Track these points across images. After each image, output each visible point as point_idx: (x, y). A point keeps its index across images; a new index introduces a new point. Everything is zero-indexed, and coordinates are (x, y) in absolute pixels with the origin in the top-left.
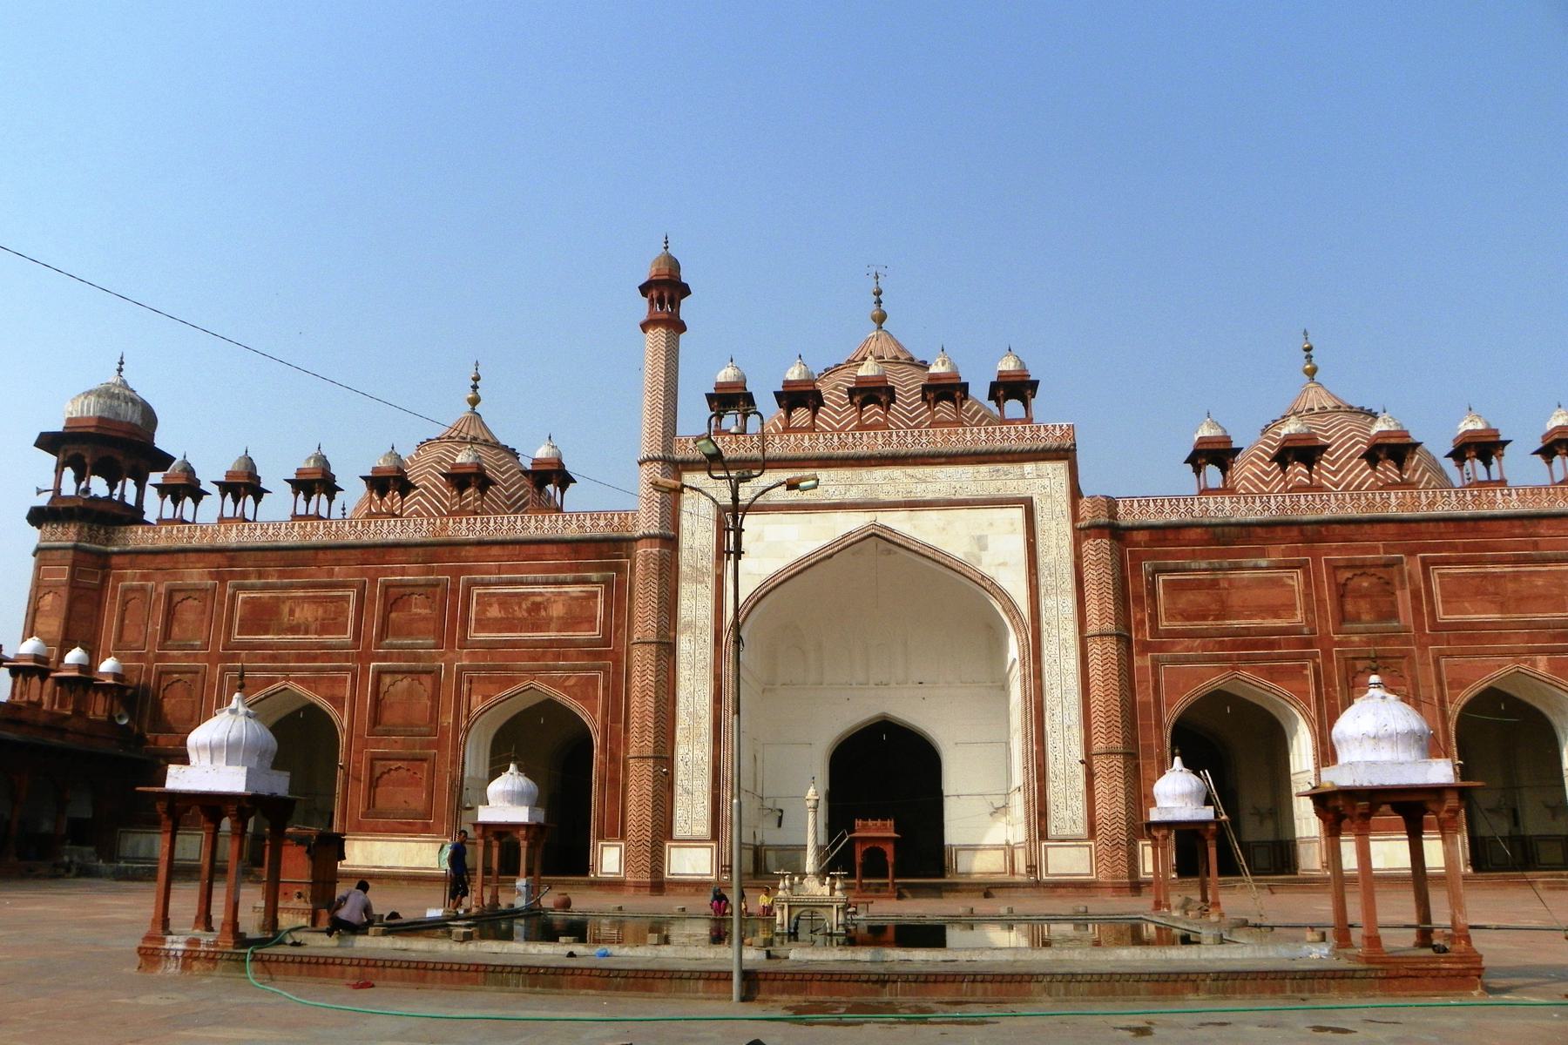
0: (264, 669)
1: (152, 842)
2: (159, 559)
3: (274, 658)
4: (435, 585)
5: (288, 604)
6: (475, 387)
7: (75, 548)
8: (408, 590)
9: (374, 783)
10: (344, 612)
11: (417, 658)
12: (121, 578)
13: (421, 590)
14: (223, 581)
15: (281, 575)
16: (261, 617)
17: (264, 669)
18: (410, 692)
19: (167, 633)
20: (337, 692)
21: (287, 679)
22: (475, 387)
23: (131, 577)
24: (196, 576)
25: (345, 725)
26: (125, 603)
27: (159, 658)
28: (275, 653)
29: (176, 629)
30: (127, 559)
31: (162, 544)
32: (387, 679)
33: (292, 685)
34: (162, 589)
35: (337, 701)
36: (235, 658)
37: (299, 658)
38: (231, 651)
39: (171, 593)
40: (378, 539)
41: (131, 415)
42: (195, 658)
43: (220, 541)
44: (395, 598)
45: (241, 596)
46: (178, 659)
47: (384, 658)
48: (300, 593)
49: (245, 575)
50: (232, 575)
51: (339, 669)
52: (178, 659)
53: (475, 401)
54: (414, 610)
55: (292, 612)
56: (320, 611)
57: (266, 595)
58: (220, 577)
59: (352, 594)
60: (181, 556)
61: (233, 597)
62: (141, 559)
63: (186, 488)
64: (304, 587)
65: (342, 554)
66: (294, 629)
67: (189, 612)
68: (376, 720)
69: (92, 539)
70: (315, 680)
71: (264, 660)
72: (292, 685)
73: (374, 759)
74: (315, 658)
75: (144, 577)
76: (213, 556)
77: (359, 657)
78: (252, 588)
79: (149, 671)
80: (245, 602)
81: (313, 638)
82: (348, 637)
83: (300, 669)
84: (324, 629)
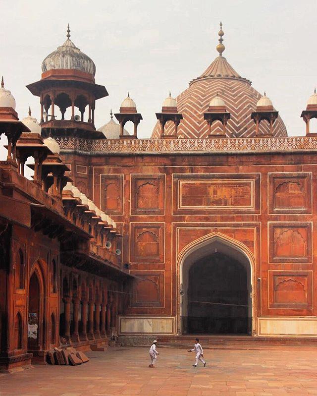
0: (203, 225)
1: (142, 324)
2: (125, 161)
3: (207, 219)
4: (304, 177)
5: (212, 188)
6: (221, 40)
7: (75, 153)
8: (286, 180)
9: (275, 288)
10: (248, 193)
11: (296, 219)
12: (101, 171)
13: (295, 180)
14: (169, 174)
15: (206, 170)
16: (195, 195)
17: (203, 225)
18: (293, 238)
19: (135, 205)
20: (249, 239)
21: (216, 231)
22: (221, 40)
23: (108, 171)
24: (150, 170)
25: (255, 256)
26: (105, 187)
27: (132, 219)
28: (207, 216)
29: (141, 202)
30: (103, 160)
31: (125, 151)
32: (278, 231)
33: (219, 234)
34: (129, 178)
35: (249, 244)
36: (182, 219)
37: (222, 219)
38: (179, 216)
39: (135, 180)
40: (266, 150)
41: (66, 64)
42: (157, 219)
43: (164, 151)
44: (280, 184)
45: (182, 183)
46: (144, 219)
47: (276, 219)
48: (219, 181)
49: (182, 170)
50: (174, 170)
51: (249, 225)
52: (142, 219)
53: (221, 50)
54: (291, 191)
55: (215, 192)
56: (233, 192)
57: (197, 182)
58: (165, 170)
59: (252, 182)
60: (140, 159)
61: (176, 184)
62: (112, 160)
63: (129, 116)
64: (222, 177)
65: (244, 159)
66: (218, 202)
67: (148, 191)
68: (273, 254)
69: (82, 147)
70: (234, 232)
71: (200, 219)
72: (219, 234)
73: (275, 275)
74: (233, 219)
75: (116, 171)
76: (159, 160)
77: (260, 218)
78: (188, 178)
79: (126, 227)
80: (184, 186)
81: (230, 207)
82: (252, 207)
83: (225, 225)
84: (236, 203)
